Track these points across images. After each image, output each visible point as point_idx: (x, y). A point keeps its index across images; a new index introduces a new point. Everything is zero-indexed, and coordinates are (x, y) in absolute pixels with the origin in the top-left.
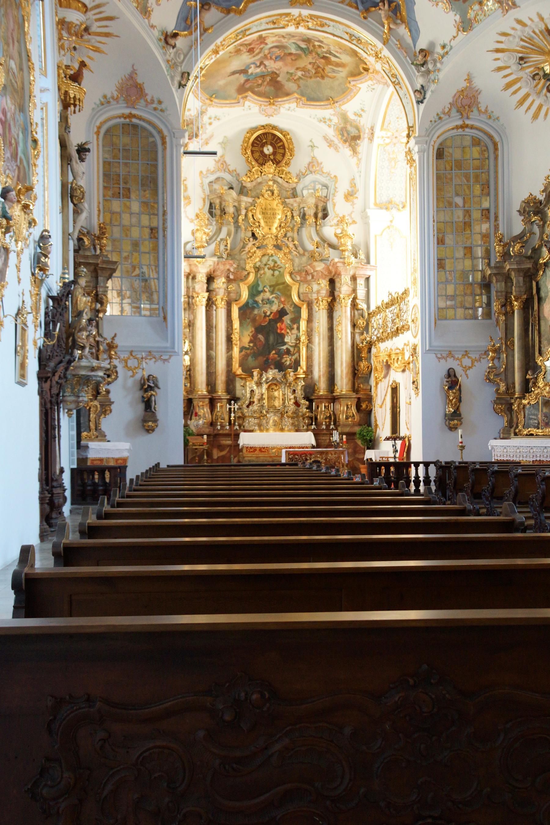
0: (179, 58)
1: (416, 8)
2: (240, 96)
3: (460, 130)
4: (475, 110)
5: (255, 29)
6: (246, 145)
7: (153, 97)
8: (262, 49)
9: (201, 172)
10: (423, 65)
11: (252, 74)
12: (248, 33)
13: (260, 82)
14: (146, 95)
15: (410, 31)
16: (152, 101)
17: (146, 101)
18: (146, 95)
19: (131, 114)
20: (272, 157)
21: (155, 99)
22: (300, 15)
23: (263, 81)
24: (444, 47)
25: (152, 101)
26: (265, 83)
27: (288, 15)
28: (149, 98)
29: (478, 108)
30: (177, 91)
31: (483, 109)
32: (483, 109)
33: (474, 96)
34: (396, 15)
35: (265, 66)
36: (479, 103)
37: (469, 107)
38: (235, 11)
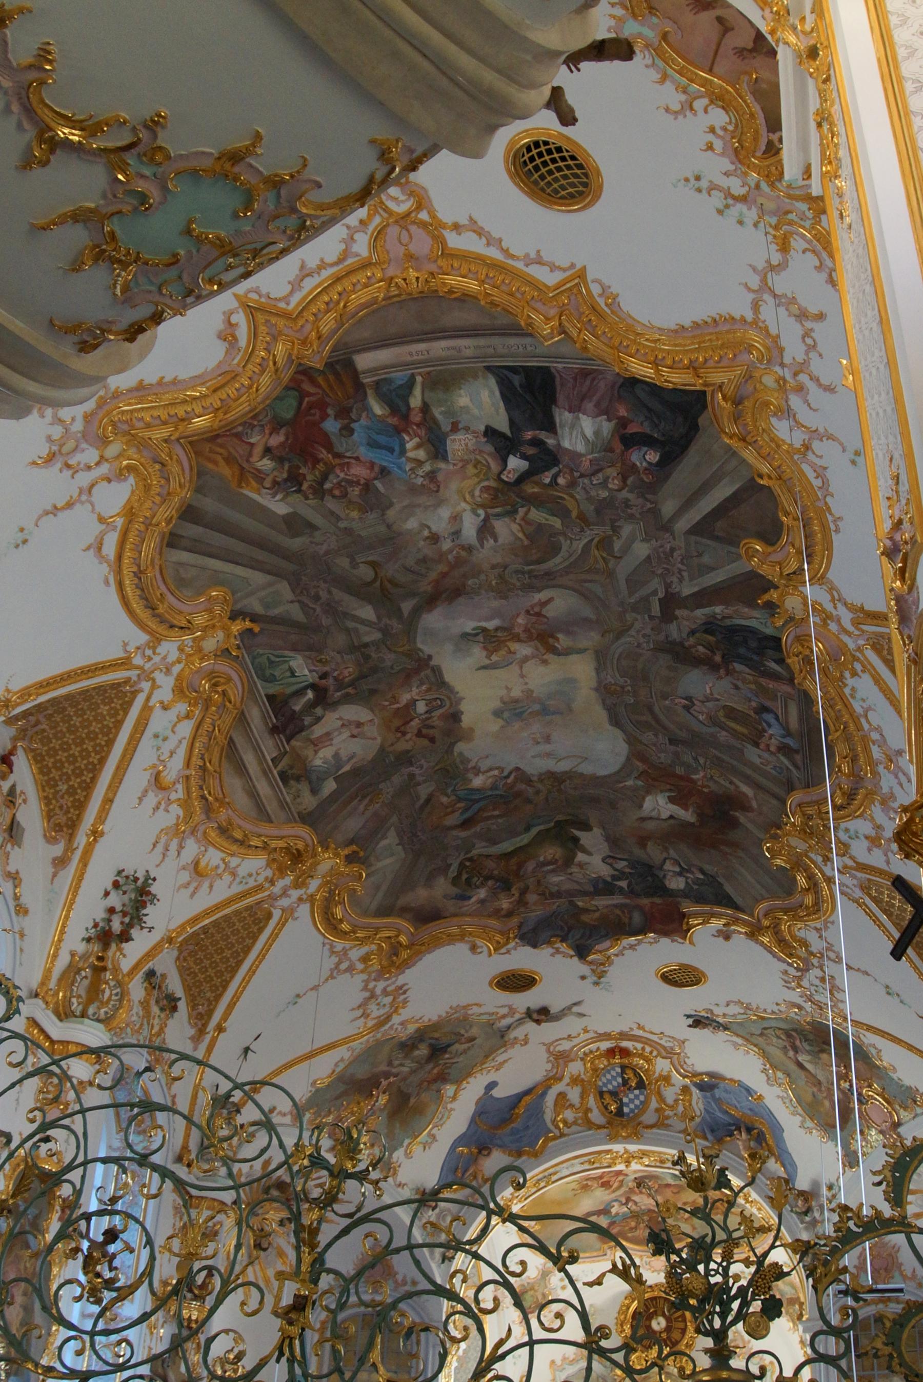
0: (444, 1220)
1: (785, 1135)
2: (606, 1246)
3: (881, 1306)
4: (897, 1274)
5: (565, 1172)
6: (622, 1317)
7: (405, 1277)
8: (622, 1181)
9: (553, 1362)
10: (806, 1213)
11: (617, 1214)
12: (554, 1178)
13: (633, 1224)
14: (396, 1273)
15: (783, 1165)
16: (404, 1283)
17: (396, 1282)
18: (396, 1273)
19: (373, 1300)
20: (664, 1335)
21: (409, 1281)
22: (626, 1151)
23: (638, 1223)
24: (830, 1188)
25: (404, 1283)
26: (642, 1225)
27: (608, 1152)
28: (399, 1277)
29: (901, 1274)
30: (439, 1267)
31: (909, 1275)
32: (909, 1275)
33: (890, 1255)
34: (761, 1144)
35: (636, 1203)
36: (901, 1264)
37: (886, 1270)
38: (528, 1154)
